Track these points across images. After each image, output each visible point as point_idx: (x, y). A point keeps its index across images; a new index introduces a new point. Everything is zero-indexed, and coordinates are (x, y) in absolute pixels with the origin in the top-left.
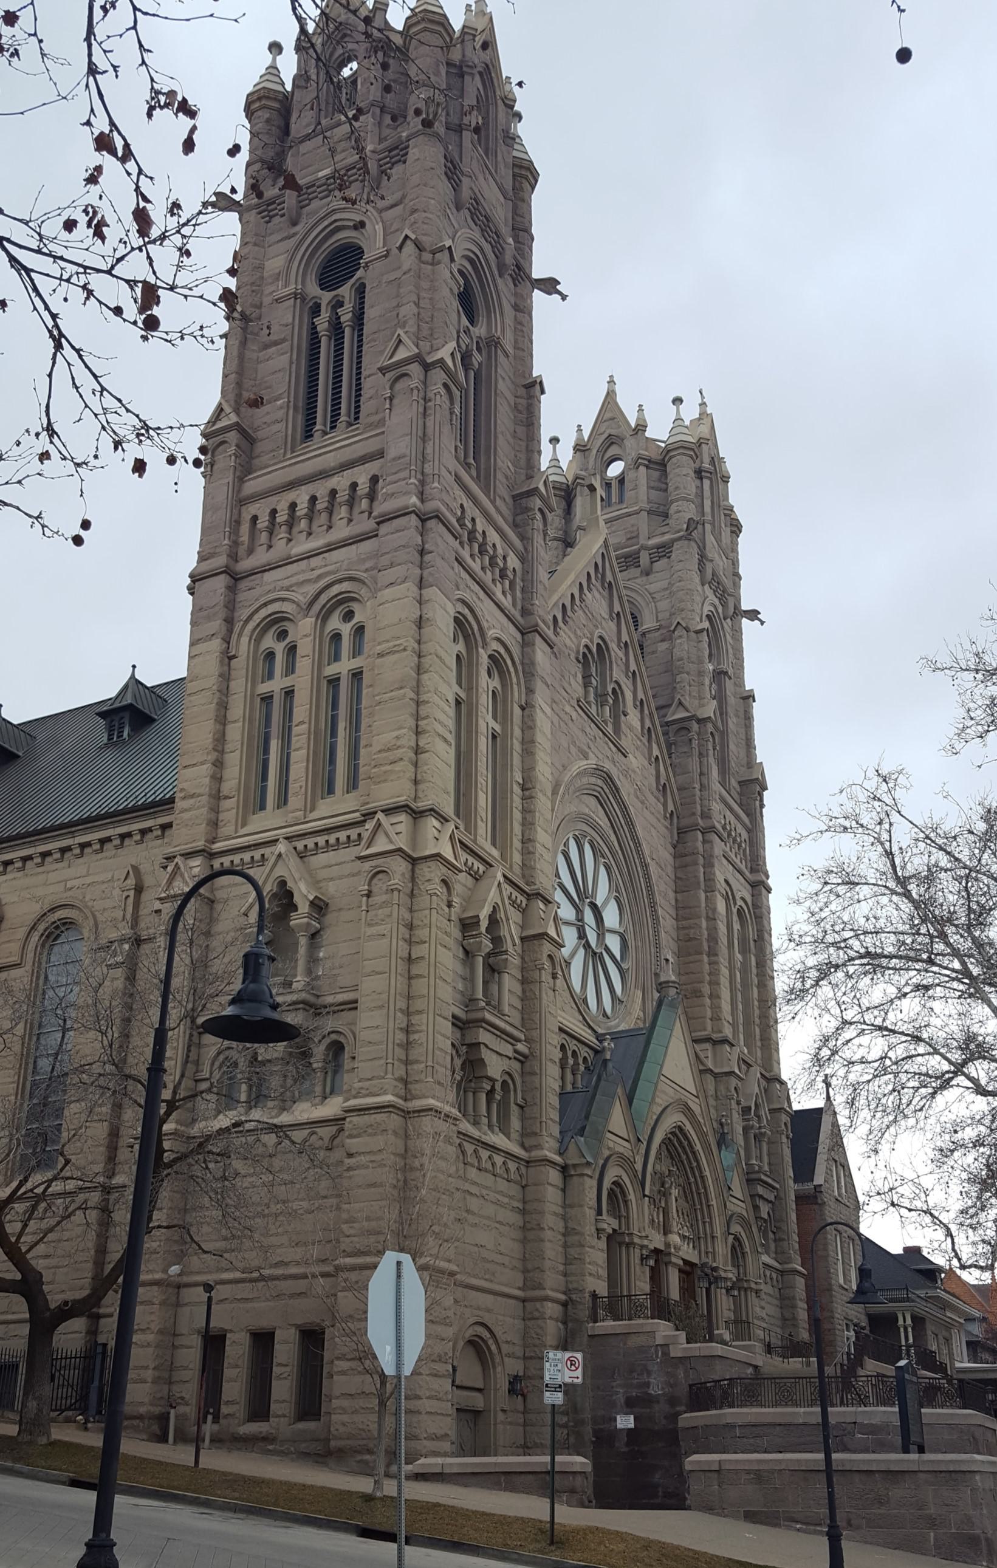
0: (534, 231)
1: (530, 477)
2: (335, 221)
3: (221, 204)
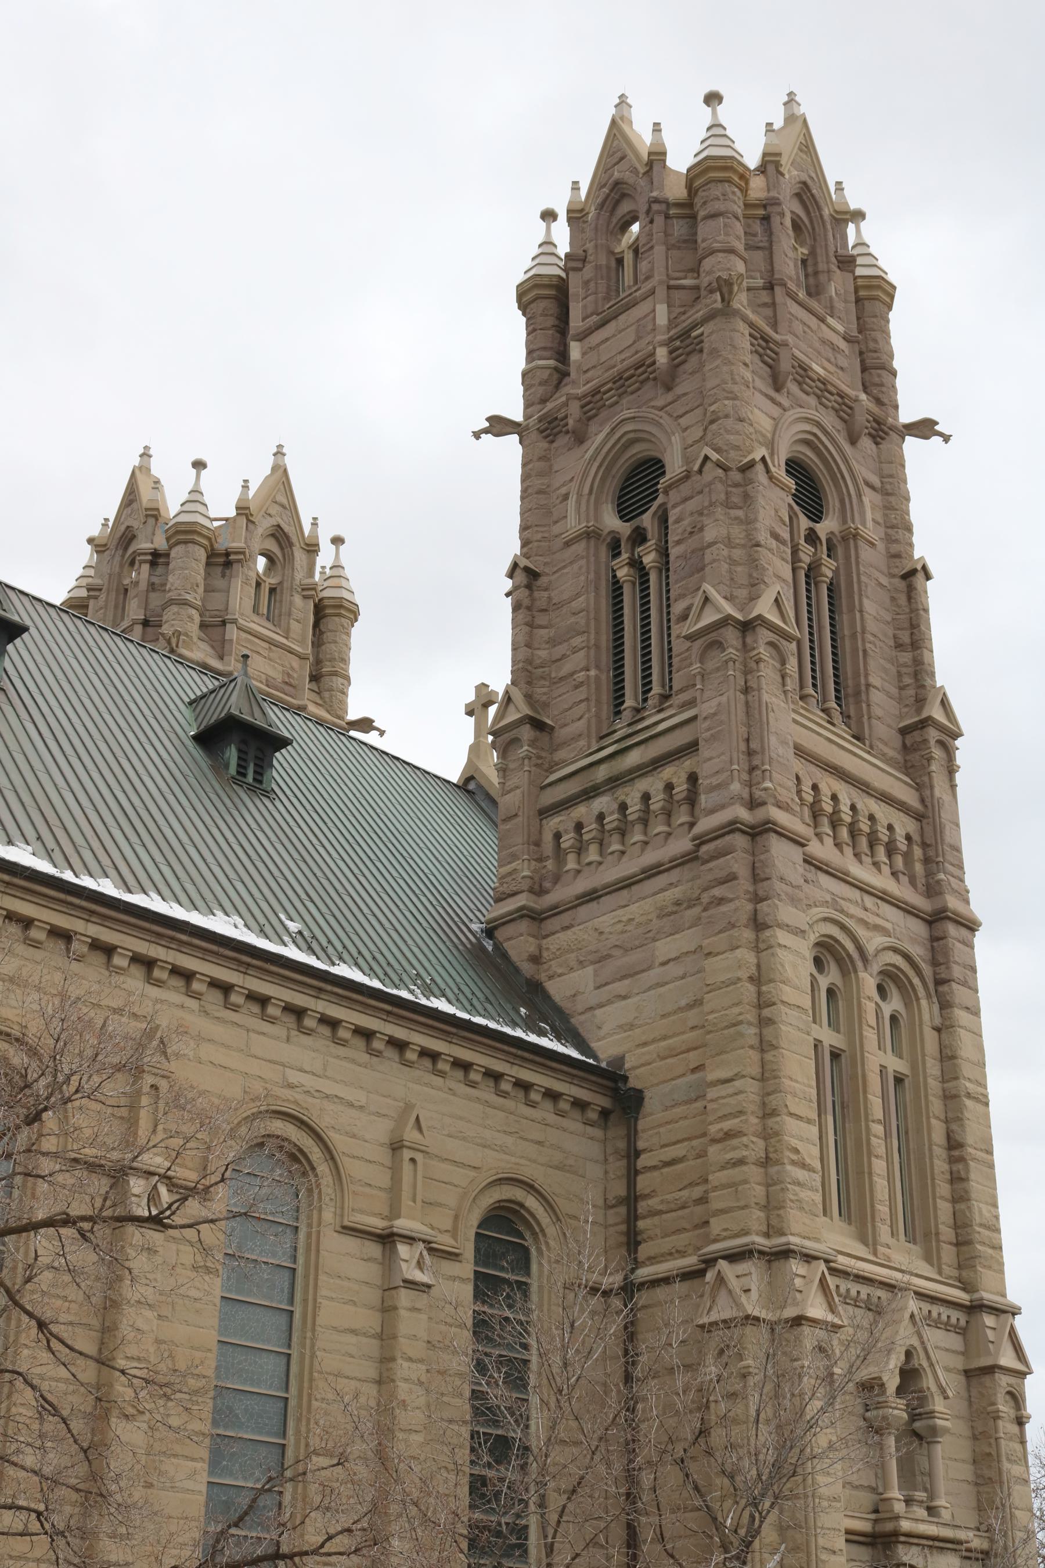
0: (896, 364)
1: (920, 702)
2: (626, 433)
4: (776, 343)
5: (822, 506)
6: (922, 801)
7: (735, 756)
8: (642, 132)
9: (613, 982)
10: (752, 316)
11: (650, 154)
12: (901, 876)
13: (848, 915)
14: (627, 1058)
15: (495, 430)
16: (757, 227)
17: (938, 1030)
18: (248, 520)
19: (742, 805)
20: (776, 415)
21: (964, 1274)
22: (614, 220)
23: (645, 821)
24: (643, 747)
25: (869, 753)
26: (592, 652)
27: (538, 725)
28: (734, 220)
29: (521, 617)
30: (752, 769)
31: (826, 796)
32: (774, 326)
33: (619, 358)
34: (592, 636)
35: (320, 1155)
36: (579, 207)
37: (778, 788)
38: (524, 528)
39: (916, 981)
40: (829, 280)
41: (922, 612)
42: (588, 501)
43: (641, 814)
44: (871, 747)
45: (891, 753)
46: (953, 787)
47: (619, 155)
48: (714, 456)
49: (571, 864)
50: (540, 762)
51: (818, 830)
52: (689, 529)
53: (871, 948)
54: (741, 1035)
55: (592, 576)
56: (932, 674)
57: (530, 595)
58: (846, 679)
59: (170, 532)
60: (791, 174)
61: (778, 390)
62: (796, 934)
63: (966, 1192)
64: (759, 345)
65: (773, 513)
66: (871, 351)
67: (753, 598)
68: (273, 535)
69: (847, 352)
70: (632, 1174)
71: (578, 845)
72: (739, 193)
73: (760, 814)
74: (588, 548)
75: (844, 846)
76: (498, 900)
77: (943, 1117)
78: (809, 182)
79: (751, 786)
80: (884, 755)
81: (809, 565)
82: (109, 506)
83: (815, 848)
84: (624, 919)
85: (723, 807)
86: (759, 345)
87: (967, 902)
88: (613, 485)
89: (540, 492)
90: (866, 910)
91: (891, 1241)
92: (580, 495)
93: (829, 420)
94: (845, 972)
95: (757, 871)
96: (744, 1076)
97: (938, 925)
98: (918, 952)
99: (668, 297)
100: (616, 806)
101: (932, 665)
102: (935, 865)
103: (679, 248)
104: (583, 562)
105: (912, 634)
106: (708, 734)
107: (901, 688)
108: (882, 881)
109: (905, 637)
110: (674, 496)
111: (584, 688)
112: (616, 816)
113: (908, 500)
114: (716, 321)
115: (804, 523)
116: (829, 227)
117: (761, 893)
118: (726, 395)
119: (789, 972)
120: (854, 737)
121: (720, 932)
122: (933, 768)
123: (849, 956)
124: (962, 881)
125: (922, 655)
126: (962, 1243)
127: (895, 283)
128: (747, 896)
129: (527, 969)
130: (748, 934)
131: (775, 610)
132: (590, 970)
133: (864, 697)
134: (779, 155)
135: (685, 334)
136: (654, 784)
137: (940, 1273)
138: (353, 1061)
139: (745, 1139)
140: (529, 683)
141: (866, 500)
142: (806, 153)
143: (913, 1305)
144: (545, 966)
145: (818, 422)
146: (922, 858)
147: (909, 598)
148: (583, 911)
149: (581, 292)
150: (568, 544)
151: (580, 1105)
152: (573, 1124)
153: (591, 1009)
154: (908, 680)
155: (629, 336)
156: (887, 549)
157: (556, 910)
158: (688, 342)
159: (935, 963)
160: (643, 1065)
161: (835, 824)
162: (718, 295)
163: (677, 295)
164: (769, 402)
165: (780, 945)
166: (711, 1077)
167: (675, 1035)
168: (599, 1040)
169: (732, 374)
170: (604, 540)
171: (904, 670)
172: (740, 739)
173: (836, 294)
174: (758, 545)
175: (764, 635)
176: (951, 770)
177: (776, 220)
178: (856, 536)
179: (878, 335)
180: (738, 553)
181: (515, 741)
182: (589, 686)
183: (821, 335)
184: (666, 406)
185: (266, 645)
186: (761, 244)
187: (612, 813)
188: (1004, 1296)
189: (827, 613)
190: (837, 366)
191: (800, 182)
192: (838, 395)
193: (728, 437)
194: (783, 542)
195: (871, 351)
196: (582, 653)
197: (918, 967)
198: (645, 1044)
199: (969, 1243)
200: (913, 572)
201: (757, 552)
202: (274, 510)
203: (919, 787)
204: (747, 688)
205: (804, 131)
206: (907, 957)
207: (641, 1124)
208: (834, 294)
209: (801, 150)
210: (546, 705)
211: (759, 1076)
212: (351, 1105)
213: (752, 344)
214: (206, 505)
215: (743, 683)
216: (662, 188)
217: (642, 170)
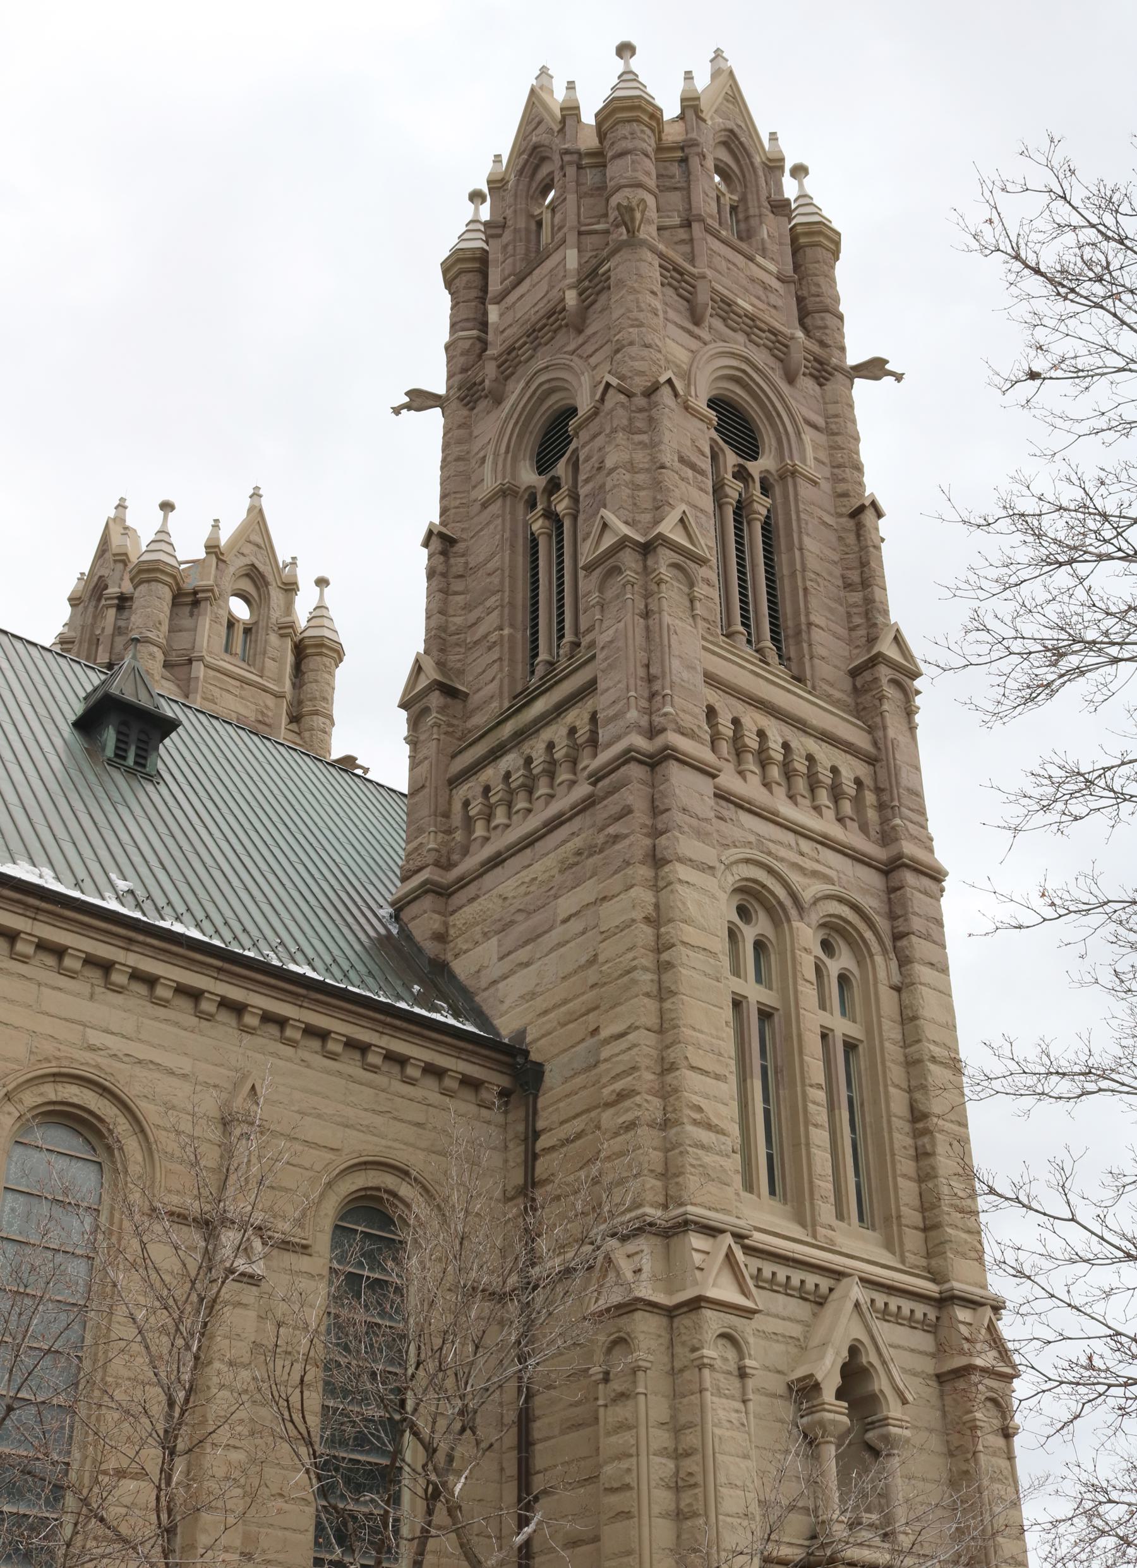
0: (842, 308)
1: (872, 640)
3: (415, 405)
4: (692, 275)
5: (758, 447)
6: (875, 743)
7: (632, 681)
8: (560, 94)
9: (516, 950)
10: (661, 247)
11: (562, 109)
12: (848, 821)
13: (777, 858)
14: (528, 1030)
15: (415, 405)
16: (675, 169)
17: (898, 989)
18: (218, 559)
19: (640, 734)
20: (694, 347)
21: (933, 1262)
22: (534, 185)
23: (551, 774)
24: (548, 694)
25: (810, 693)
26: (506, 611)
27: (449, 692)
28: (642, 156)
29: (434, 584)
30: (652, 695)
31: (750, 731)
32: (692, 261)
33: (532, 311)
34: (507, 594)
35: (127, 1126)
36: (499, 177)
37: (681, 714)
38: (444, 496)
39: (868, 935)
40: (761, 223)
41: (871, 549)
42: (505, 459)
43: (546, 766)
44: (814, 688)
45: (838, 695)
46: (912, 728)
47: (537, 120)
48: (614, 381)
49: (480, 830)
50: (451, 729)
51: (742, 767)
52: (597, 465)
53: (807, 896)
54: (634, 982)
55: (507, 535)
56: (886, 613)
57: (447, 562)
58: (785, 621)
59: (134, 572)
60: (714, 121)
61: (697, 323)
62: (703, 871)
63: (933, 1168)
64: (672, 277)
65: (689, 443)
66: (814, 295)
67: (657, 522)
68: (247, 575)
69: (781, 291)
70: (531, 1158)
71: (487, 811)
72: (648, 131)
73: (659, 741)
74: (504, 505)
75: (774, 785)
76: (403, 880)
77: (905, 1085)
78: (736, 129)
79: (651, 714)
80: (829, 696)
81: (739, 502)
82: (84, 562)
83: (729, 780)
84: (527, 879)
85: (619, 738)
86: (672, 277)
87: (931, 851)
88: (531, 442)
89: (458, 459)
90: (802, 854)
91: (835, 1223)
92: (496, 455)
93: (760, 357)
94: (776, 923)
95: (657, 803)
96: (637, 1028)
97: (895, 875)
98: (871, 903)
99: (579, 242)
100: (521, 762)
101: (885, 603)
102: (889, 810)
103: (592, 196)
104: (499, 521)
105: (862, 573)
106: (605, 664)
107: (851, 629)
108: (826, 825)
109: (855, 577)
110: (584, 435)
111: (497, 648)
112: (521, 772)
113: (857, 439)
114: (621, 253)
115: (731, 459)
116: (761, 173)
117: (660, 826)
118: (630, 322)
119: (693, 910)
120: (793, 677)
121: (616, 872)
122: (886, 707)
123: (780, 903)
124: (925, 827)
125: (872, 593)
126: (930, 1227)
127: (839, 230)
128: (645, 831)
129: (430, 948)
130: (644, 872)
131: (680, 529)
132: (494, 941)
133: (804, 636)
134: (698, 99)
135: (594, 272)
136: (557, 732)
137: (903, 1262)
138: (177, 1024)
139: (638, 1099)
140: (442, 650)
141: (806, 438)
143: (857, 1292)
144: (452, 945)
145: (746, 358)
146: (875, 804)
147: (858, 536)
148: (489, 879)
149: (500, 257)
150: (485, 505)
151: (470, 1083)
152: (464, 1104)
153: (495, 982)
154: (857, 620)
155: (544, 287)
156: (834, 488)
157: (463, 883)
158: (596, 280)
159: (892, 916)
160: (543, 1036)
161: (764, 762)
162: (623, 230)
163: (588, 240)
164: (687, 335)
165: (680, 881)
166: (605, 1033)
167: (576, 997)
168: (502, 1016)
169: (638, 302)
170: (522, 497)
171: (855, 610)
172: (638, 664)
173: (769, 236)
174: (663, 467)
175: (665, 557)
176: (909, 712)
177: (694, 162)
178: (794, 473)
179: (821, 280)
180: (641, 478)
181: (426, 710)
182: (502, 646)
183: (749, 274)
184: (577, 349)
185: (238, 683)
186: (678, 185)
187: (519, 769)
188: (984, 1287)
189: (761, 553)
190: (769, 304)
191: (726, 130)
192: (770, 331)
193: (632, 363)
194: (702, 473)
195: (814, 295)
196: (496, 612)
197: (869, 919)
198: (545, 1012)
199: (937, 1226)
200: (861, 509)
201: (660, 474)
202: (248, 549)
203: (871, 730)
204: (647, 613)
205: (731, 82)
206: (855, 907)
207: (541, 1102)
208: (766, 236)
209: (728, 101)
210: (461, 672)
211: (656, 1028)
212: (172, 1073)
213: (662, 275)
214: (171, 544)
215: (642, 607)
216: (576, 138)
217: (556, 128)
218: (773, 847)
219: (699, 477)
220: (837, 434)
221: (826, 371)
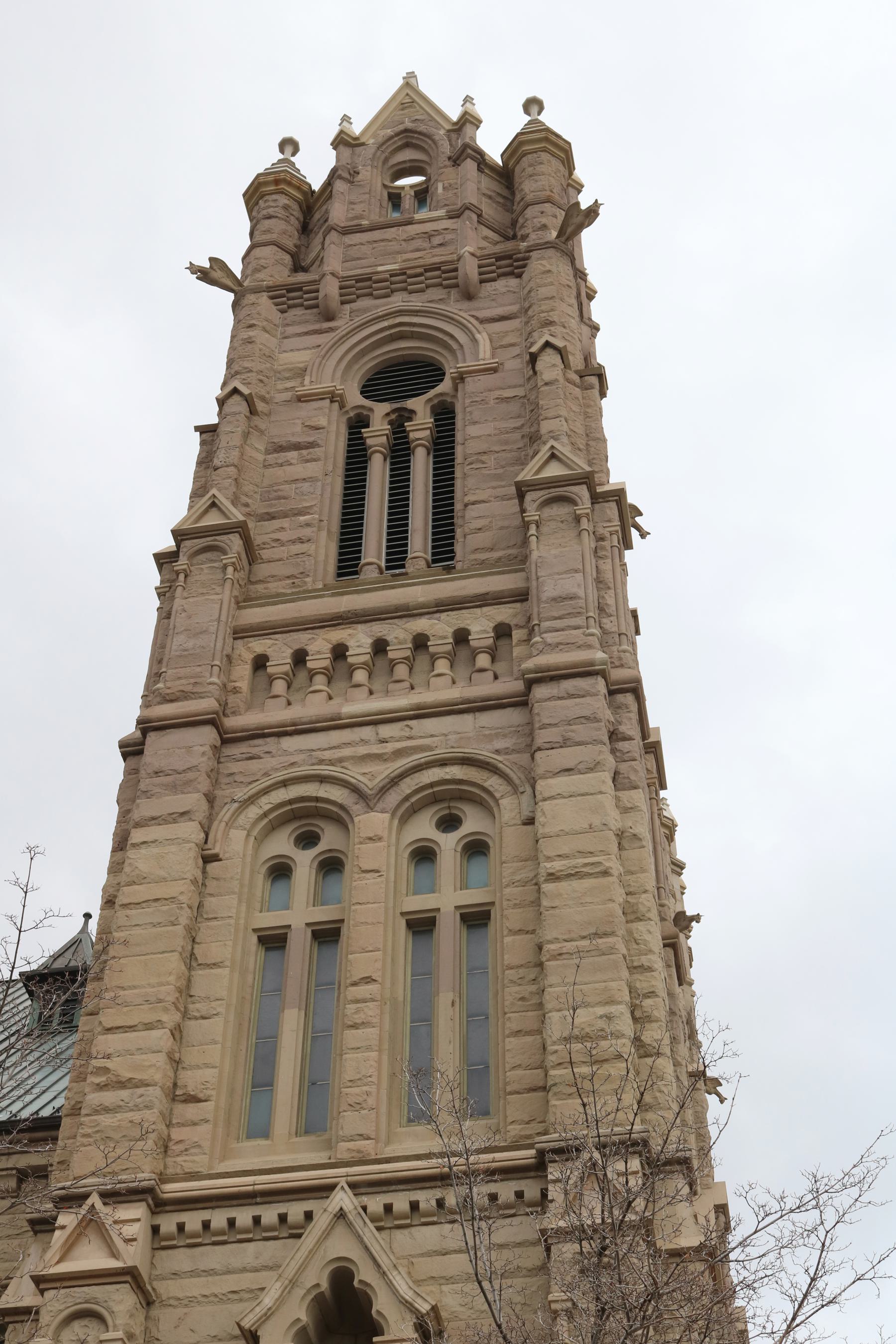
13: (331, 763)
39: (493, 782)
62: (175, 821)
90: (383, 741)
123: (342, 807)
142: (410, 107)
145: (400, 311)
173: (444, 188)
191: (397, 134)
197: (488, 763)
213: (277, 305)
218: (327, 755)
219: (304, 452)
220: (529, 307)
221: (517, 260)
